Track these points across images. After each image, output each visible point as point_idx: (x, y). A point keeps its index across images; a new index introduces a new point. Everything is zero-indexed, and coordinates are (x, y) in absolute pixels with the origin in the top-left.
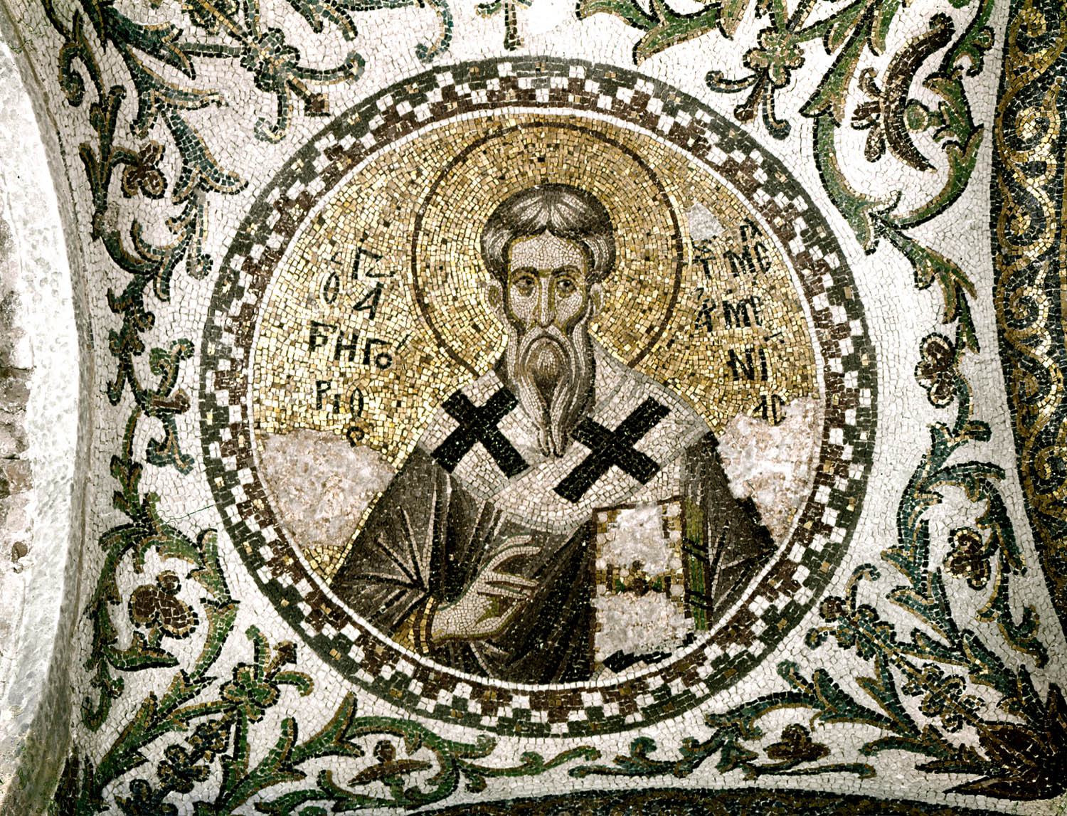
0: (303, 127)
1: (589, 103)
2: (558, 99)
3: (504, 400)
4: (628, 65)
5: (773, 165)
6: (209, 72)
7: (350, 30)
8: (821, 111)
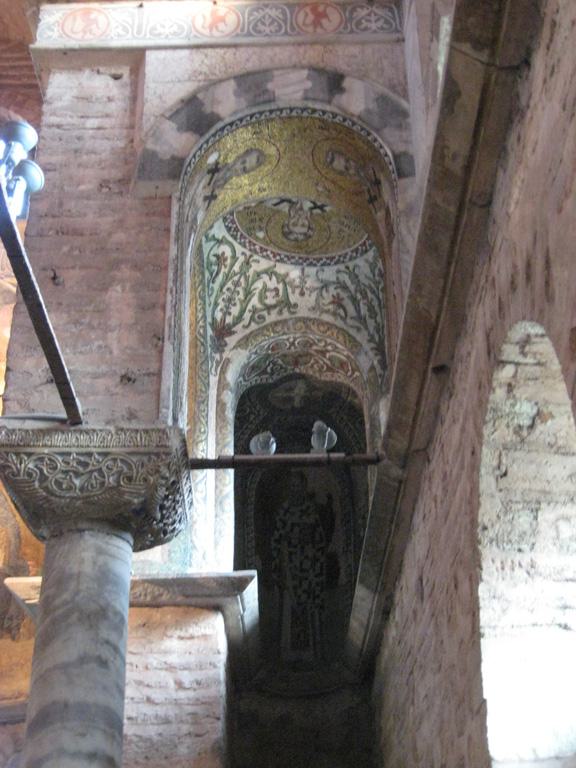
0: (351, 265)
1: (286, 256)
2: (293, 257)
3: (311, 209)
4: (278, 264)
5: (245, 246)
6: (367, 282)
7: (338, 278)
8: (234, 258)
